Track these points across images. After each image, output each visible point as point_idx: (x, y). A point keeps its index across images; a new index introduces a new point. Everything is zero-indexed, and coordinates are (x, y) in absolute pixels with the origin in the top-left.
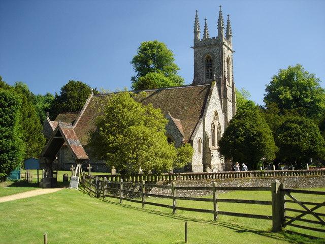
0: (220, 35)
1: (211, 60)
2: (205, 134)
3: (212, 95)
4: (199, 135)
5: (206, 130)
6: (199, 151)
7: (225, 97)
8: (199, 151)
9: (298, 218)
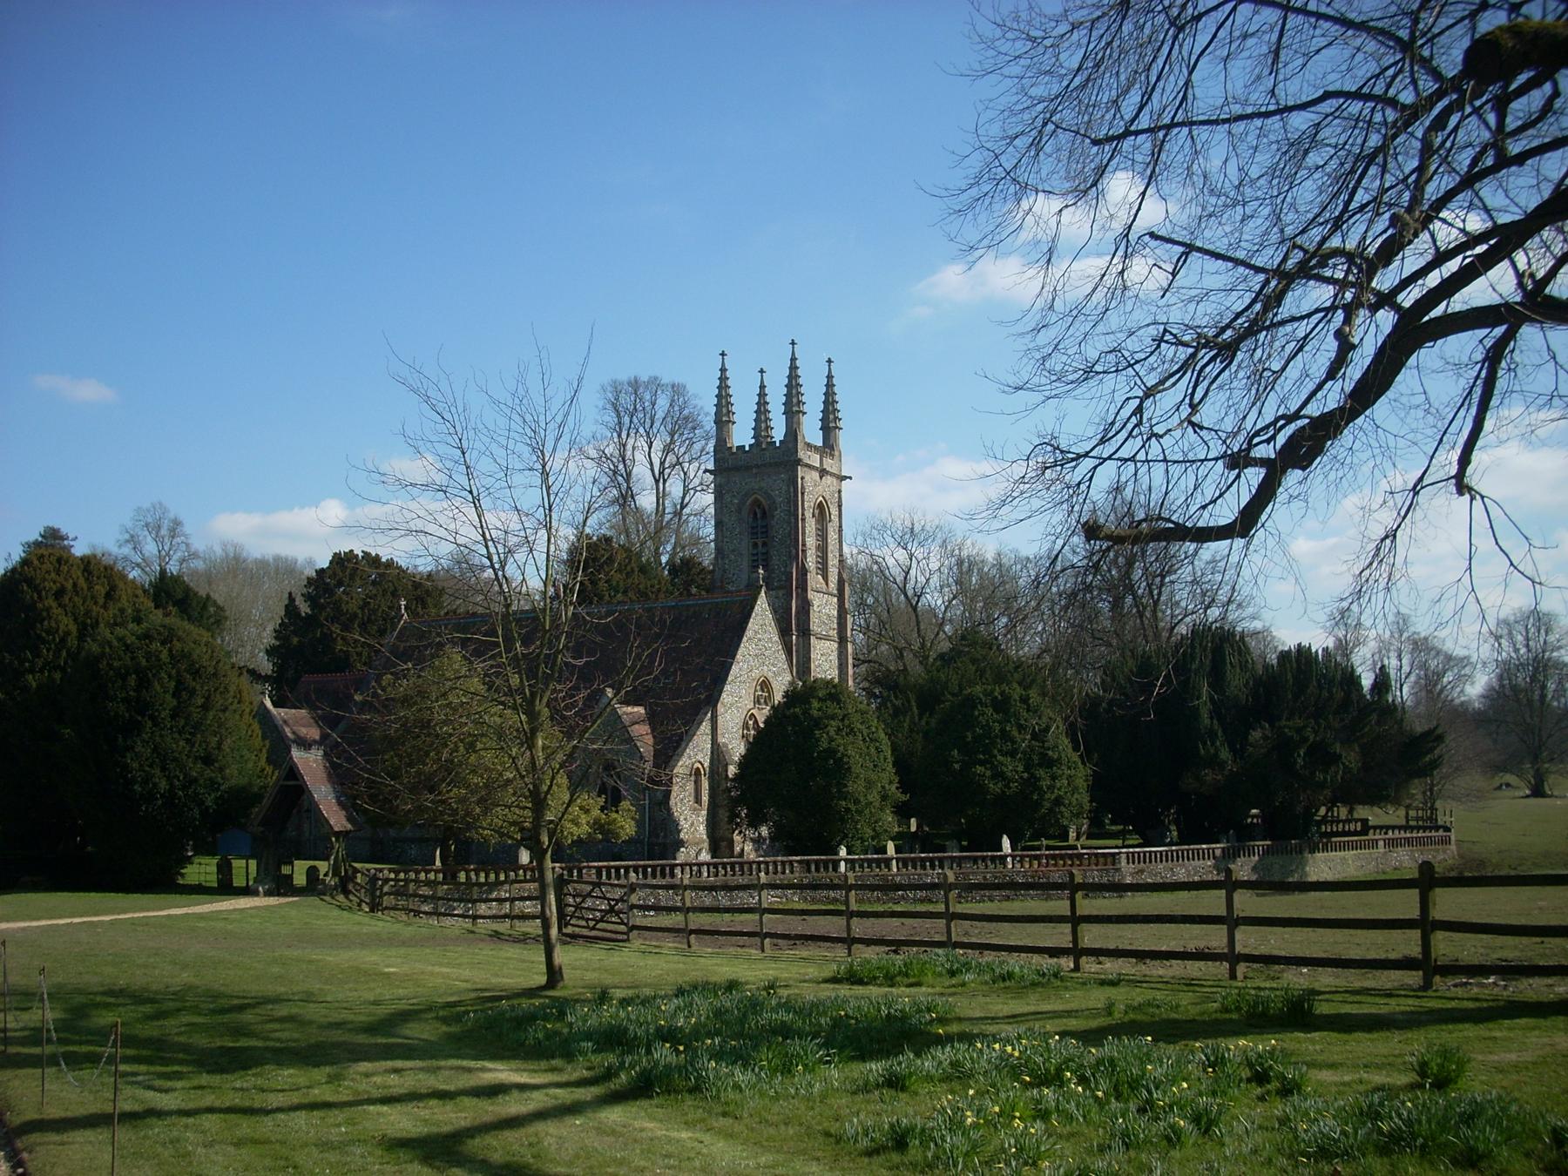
0: (792, 433)
1: (764, 513)
2: (717, 753)
3: (749, 633)
4: (697, 753)
5: (721, 740)
6: (698, 800)
7: (805, 632)
8: (698, 800)
9: (602, 920)
